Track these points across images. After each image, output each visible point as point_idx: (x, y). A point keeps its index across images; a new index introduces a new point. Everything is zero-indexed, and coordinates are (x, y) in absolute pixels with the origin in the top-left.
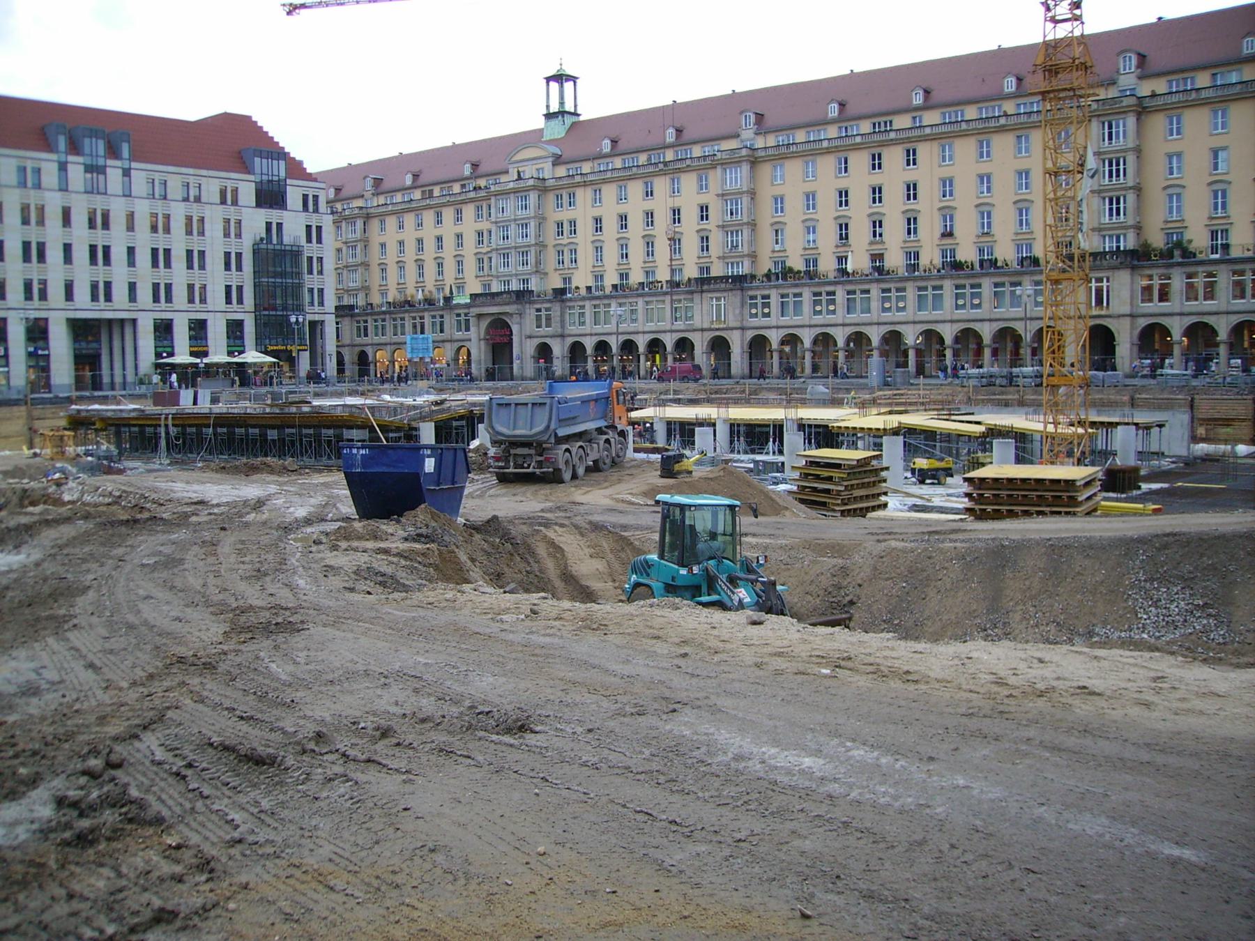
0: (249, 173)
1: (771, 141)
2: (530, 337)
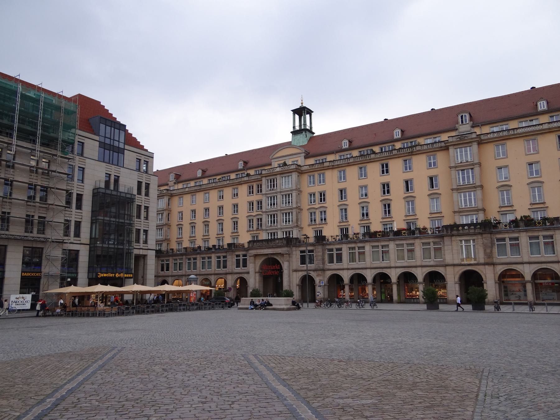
0: (95, 134)
1: (486, 129)
2: (296, 271)
